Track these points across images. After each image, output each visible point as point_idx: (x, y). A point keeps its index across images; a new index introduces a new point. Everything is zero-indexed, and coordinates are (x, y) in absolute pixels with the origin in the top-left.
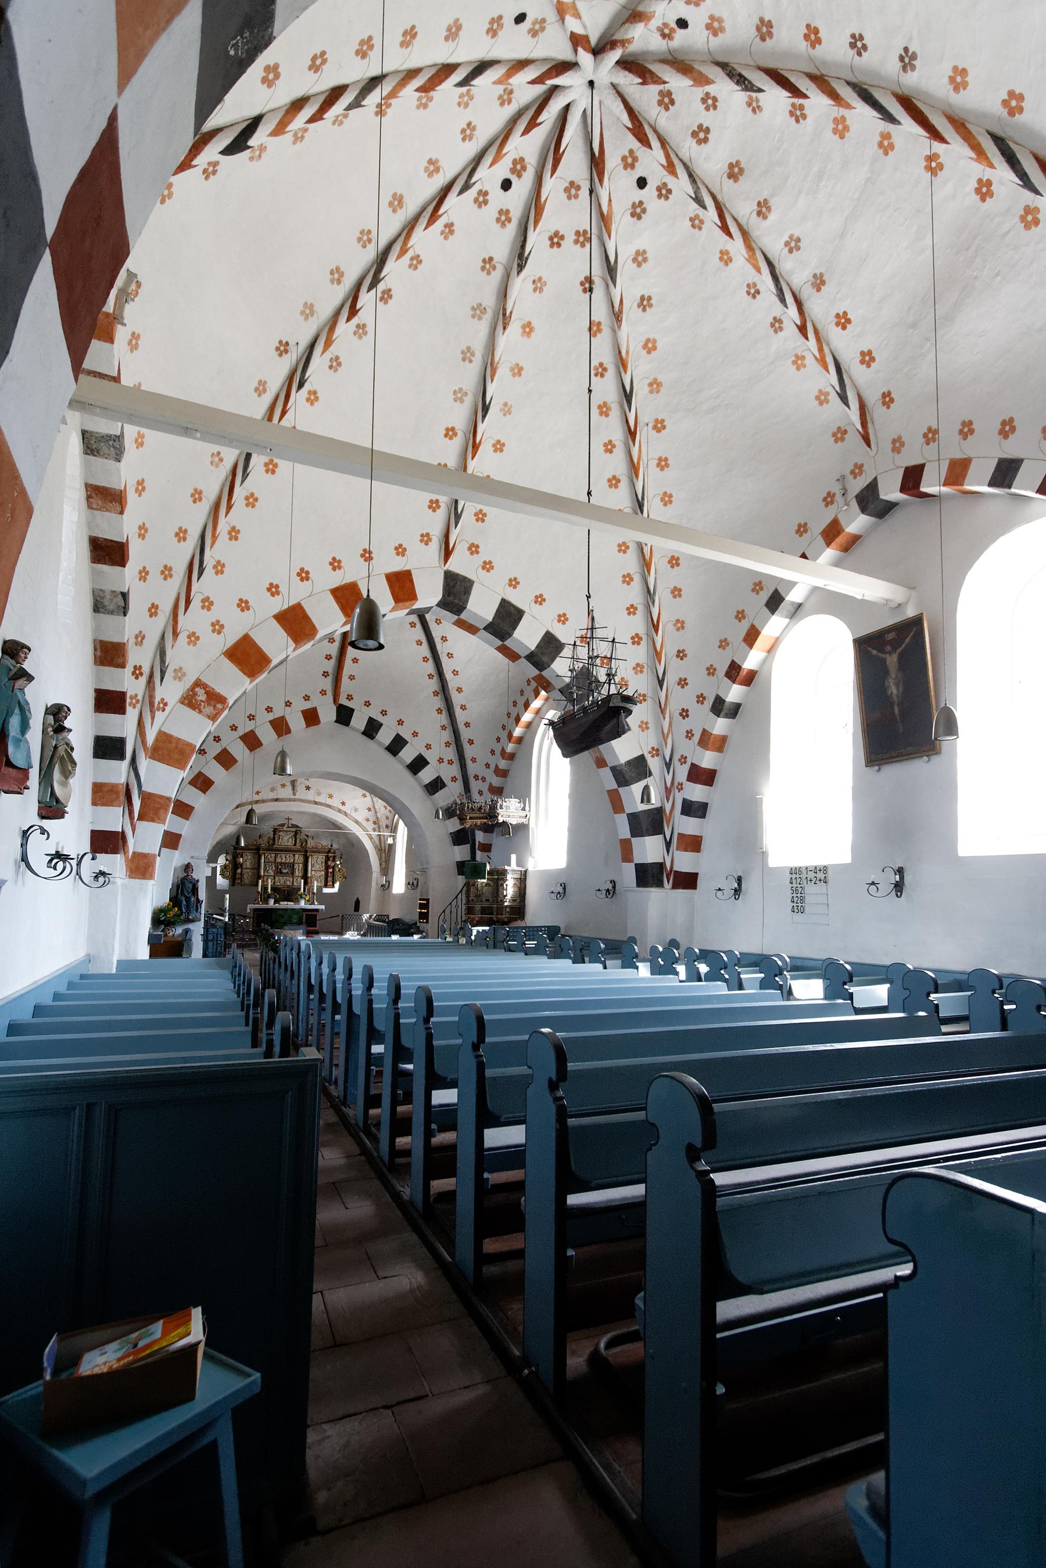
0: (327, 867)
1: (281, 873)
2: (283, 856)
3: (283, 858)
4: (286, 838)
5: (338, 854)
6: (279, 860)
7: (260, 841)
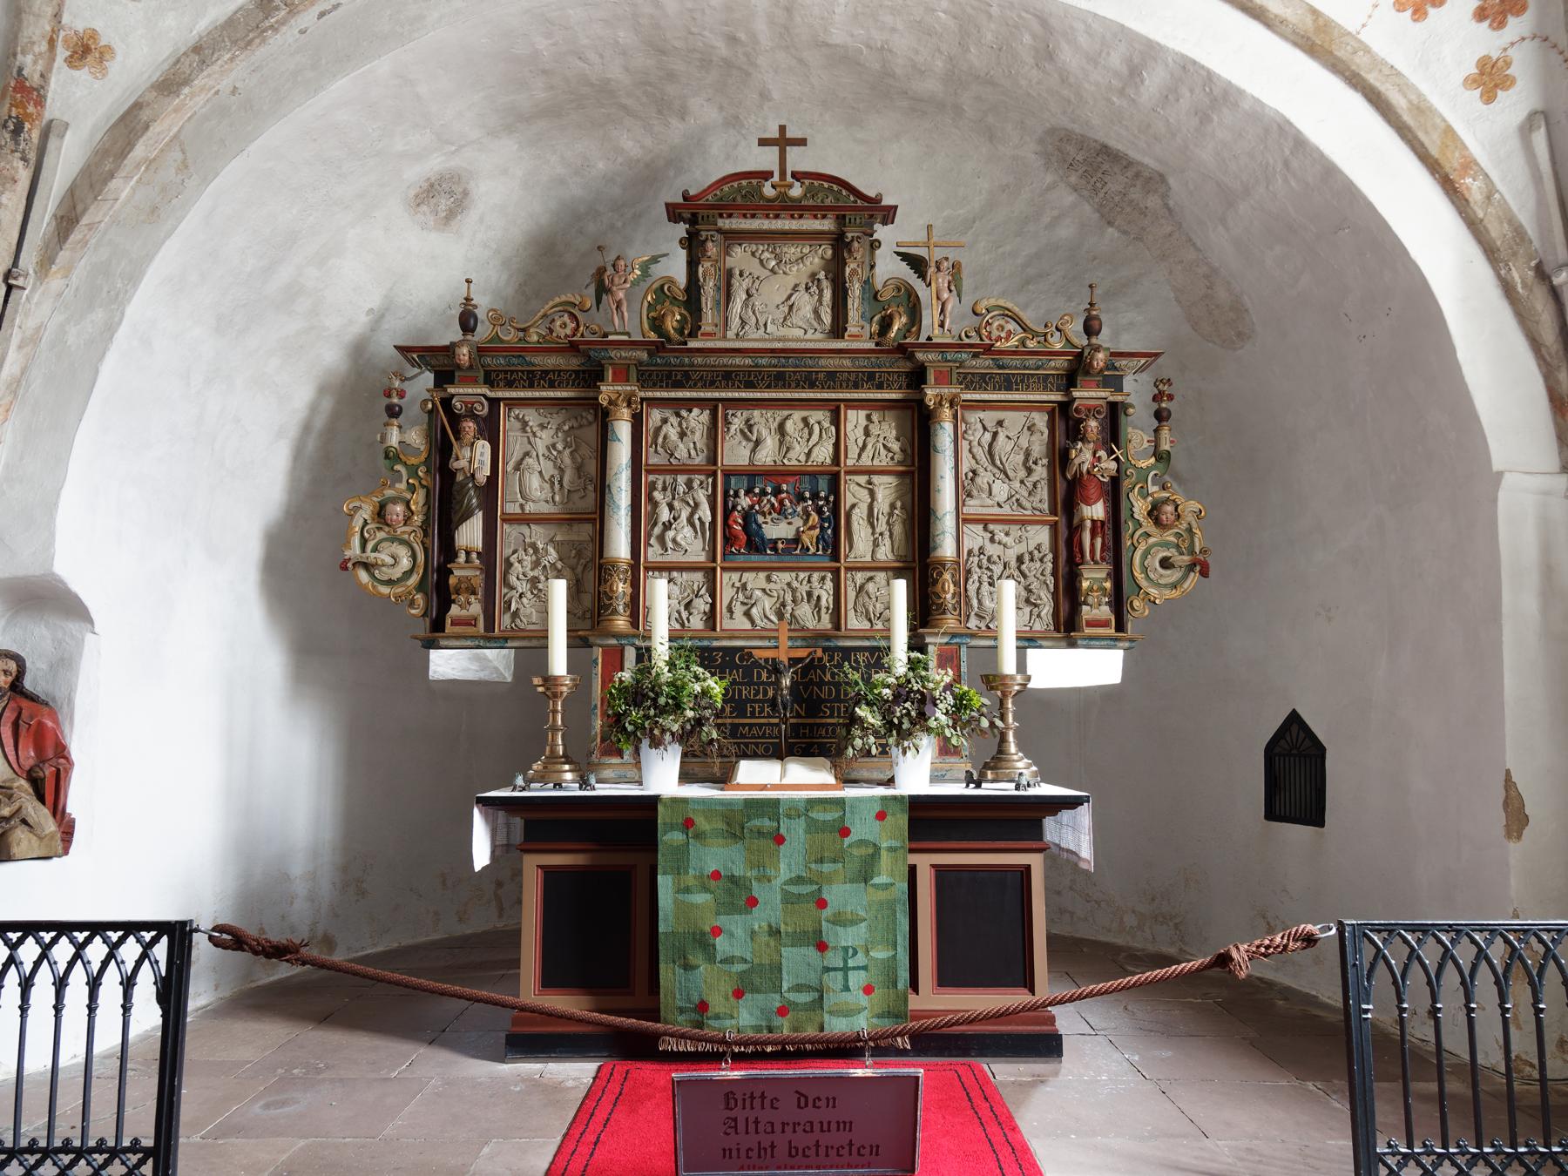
0: (1068, 492)
1: (756, 543)
2: (764, 422)
3: (772, 438)
4: (773, 292)
5: (1136, 389)
6: (735, 453)
7: (595, 322)
